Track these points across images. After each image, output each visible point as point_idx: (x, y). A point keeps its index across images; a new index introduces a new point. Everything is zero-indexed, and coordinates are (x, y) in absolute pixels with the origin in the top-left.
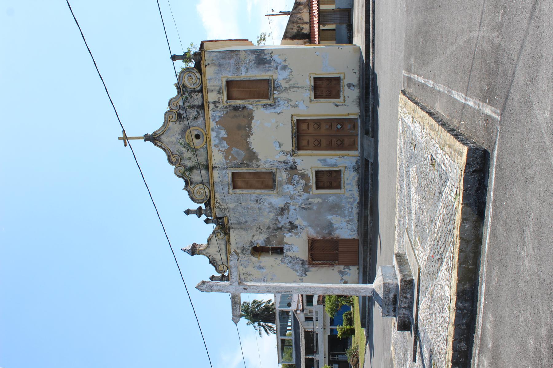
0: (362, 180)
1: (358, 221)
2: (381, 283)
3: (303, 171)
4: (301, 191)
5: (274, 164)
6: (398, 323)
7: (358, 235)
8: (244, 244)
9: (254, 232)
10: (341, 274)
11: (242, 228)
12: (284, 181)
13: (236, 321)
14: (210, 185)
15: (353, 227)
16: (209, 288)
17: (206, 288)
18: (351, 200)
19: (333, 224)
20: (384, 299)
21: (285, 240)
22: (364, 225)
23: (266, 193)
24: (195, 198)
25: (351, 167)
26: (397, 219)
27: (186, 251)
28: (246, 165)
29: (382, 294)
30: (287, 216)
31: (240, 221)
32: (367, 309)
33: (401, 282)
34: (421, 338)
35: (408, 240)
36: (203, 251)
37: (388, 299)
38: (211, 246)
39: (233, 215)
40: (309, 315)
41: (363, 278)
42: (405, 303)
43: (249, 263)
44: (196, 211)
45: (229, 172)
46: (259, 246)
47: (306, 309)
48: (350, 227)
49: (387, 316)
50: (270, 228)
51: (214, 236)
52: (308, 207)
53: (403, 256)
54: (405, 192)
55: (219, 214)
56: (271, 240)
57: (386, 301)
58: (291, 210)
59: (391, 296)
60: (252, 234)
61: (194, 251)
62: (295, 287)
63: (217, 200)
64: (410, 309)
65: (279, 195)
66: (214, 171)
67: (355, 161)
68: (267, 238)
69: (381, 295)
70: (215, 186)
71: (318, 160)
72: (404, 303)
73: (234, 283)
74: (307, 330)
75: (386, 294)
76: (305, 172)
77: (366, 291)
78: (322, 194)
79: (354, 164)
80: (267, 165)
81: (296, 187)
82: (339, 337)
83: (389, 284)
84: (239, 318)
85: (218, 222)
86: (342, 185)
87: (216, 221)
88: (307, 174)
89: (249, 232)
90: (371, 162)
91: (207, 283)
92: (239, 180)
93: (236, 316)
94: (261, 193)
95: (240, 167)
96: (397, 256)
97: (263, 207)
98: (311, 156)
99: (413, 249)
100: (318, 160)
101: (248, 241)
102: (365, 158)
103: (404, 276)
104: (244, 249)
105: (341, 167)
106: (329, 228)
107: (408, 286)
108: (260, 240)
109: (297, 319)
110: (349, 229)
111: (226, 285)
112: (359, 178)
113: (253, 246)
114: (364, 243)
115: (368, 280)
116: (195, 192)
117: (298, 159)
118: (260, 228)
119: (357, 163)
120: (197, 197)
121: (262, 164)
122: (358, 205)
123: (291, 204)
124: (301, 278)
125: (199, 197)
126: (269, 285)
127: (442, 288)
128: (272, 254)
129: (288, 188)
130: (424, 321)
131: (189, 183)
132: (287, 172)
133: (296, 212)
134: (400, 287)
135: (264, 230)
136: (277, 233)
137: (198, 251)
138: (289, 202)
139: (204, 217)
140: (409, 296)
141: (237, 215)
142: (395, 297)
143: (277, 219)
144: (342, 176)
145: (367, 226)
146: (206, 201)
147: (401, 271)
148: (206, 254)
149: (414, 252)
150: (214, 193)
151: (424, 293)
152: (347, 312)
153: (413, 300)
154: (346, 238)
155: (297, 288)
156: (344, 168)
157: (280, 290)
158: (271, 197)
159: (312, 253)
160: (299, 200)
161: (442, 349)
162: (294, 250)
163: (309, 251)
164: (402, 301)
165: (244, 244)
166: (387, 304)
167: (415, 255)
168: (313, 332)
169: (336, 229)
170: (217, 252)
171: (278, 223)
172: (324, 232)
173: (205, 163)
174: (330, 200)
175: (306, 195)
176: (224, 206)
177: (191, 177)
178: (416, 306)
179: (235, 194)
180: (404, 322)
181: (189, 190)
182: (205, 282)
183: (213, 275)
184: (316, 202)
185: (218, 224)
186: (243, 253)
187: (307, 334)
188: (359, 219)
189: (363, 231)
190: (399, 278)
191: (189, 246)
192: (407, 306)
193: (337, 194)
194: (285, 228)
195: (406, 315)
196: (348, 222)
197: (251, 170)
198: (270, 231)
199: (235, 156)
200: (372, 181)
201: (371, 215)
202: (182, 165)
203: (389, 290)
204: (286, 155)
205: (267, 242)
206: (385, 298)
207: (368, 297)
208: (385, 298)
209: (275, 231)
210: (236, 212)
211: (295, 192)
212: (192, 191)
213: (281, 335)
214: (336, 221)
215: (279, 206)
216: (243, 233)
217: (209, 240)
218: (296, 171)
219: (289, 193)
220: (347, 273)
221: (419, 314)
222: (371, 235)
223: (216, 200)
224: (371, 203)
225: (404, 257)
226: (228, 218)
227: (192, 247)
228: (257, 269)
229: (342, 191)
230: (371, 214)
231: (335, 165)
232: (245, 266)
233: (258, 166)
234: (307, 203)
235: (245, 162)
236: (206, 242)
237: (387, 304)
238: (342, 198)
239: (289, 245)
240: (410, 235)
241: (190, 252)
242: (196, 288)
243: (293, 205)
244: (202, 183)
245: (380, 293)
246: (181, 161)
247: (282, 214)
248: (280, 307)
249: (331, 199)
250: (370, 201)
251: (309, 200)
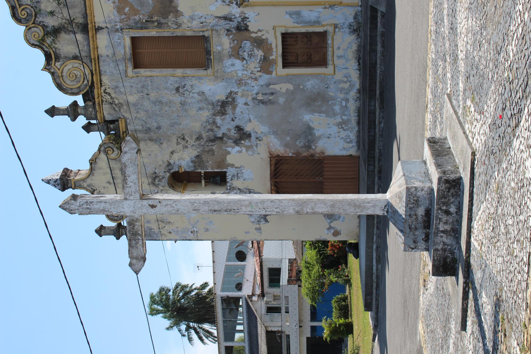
0: (364, 47)
1: (358, 123)
2: (403, 187)
3: (259, 34)
4: (256, 70)
5: (208, 21)
6: (434, 261)
7: (359, 148)
8: (155, 168)
9: (173, 146)
10: (329, 219)
11: (151, 140)
12: (225, 52)
13: (136, 267)
14: (91, 61)
15: (350, 134)
16: (85, 206)
17: (80, 206)
18: (346, 86)
19: (313, 129)
20: (408, 217)
21: (230, 159)
22: (369, 128)
23: (193, 75)
24: (65, 86)
25: (346, 26)
26: (430, 90)
27: (52, 182)
28: (156, 24)
29: (404, 209)
30: (232, 116)
31: (148, 126)
32: (374, 277)
33: (439, 184)
34: (476, 282)
35: (452, 111)
36: (81, 183)
37: (414, 217)
38: (96, 173)
39: (135, 115)
40: (274, 304)
41: (367, 223)
42: (446, 223)
44: (67, 109)
45: (126, 37)
46: (183, 170)
47: (267, 293)
48: (343, 134)
49: (413, 249)
50: (202, 138)
51: (102, 153)
52: (270, 100)
53: (441, 143)
54: (445, 30)
55: (109, 114)
56: (203, 159)
57: (412, 222)
58: (239, 105)
59: (421, 211)
60: (171, 150)
61: (65, 181)
62: (244, 200)
63: (106, 89)
64: (455, 235)
65: (216, 77)
66: (98, 36)
67: (353, 14)
68: (197, 157)
69: (402, 210)
70: (101, 64)
71: (286, 12)
72: (444, 223)
73: (131, 195)
74: (270, 329)
75: (411, 208)
76: (263, 35)
77: (374, 206)
78: (294, 75)
79: (351, 20)
80: (194, 23)
81: (247, 63)
82: (326, 339)
83: (416, 188)
84: (142, 263)
85: (108, 128)
86: (329, 58)
87: (105, 127)
88: (267, 39)
89: (164, 145)
90: (382, 12)
91: (82, 197)
92: (144, 51)
93: (137, 258)
94: (185, 75)
95: (146, 28)
96: (430, 142)
97: (189, 101)
98: (274, 5)
99: (460, 123)
100: (286, 12)
101: (163, 162)
102: (370, 5)
103: (444, 172)
104: (156, 177)
105: (327, 25)
106: (306, 136)
107: (452, 191)
108: (184, 160)
109: (253, 311)
110: (342, 138)
111: (116, 201)
112: (359, 46)
113: (172, 171)
114: (368, 161)
115: (375, 225)
116: (64, 74)
117: (250, 13)
118: (184, 139)
119: (355, 17)
120: (68, 83)
121: (185, 21)
122: (358, 95)
123: (239, 94)
124: (258, 226)
125: (72, 84)
126: (197, 197)
127: (520, 166)
128: (205, 186)
129: (233, 65)
130: (483, 247)
131: (53, 57)
132: (231, 37)
133: (247, 109)
134: (437, 192)
135: (191, 142)
136: (214, 148)
137: (73, 183)
138: (235, 90)
139: (82, 120)
140: (453, 209)
141: (142, 115)
142: (428, 213)
143: (214, 123)
144: (330, 42)
145: (375, 128)
146: (85, 91)
147: (438, 165)
148: (88, 188)
149: (463, 128)
150: (100, 75)
151: (482, 197)
152: (340, 296)
153: (461, 217)
154: (337, 154)
155: (247, 203)
156: (333, 27)
157: (216, 208)
158: (203, 81)
159: (276, 182)
160: (254, 86)
161: (519, 283)
162: (245, 176)
163: (271, 178)
164: (440, 219)
165: (155, 168)
166: (413, 226)
167: (465, 133)
168: (281, 332)
169: (320, 137)
170: (109, 182)
171: (216, 129)
172: (297, 143)
173: (81, 20)
174: (309, 87)
175: (265, 78)
176: (120, 99)
177: (56, 46)
178: (468, 225)
179: (137, 76)
180: (445, 259)
181: (52, 71)
182: (78, 196)
183: (102, 226)
184: (284, 90)
185: (107, 133)
186: (154, 184)
187: (271, 336)
188: (359, 119)
189: (367, 139)
190: (435, 175)
191: (56, 173)
192: (449, 229)
193: (319, 74)
194: (229, 138)
195: (448, 245)
196: (341, 125)
197: (166, 33)
198: (202, 144)
199: (136, 7)
200: (383, 46)
201: (380, 109)
202: (39, 25)
203: (417, 201)
204: (229, 5)
205: (197, 164)
206: (410, 215)
207: (378, 216)
208: (410, 215)
209: (211, 144)
210: (139, 110)
211: (245, 72)
212: (59, 72)
213: (226, 340)
214: (319, 123)
215: (217, 98)
216: (154, 147)
217: (93, 162)
218: (246, 33)
219: (235, 74)
220: (339, 217)
221: (472, 239)
222: (381, 144)
223: (103, 88)
224: (380, 87)
225: (444, 143)
226: (126, 122)
227: (62, 175)
229: (329, 70)
230: (382, 107)
231: (317, 23)
233: (179, 25)
234: (267, 92)
235: (155, 18)
236: (88, 167)
237: (413, 226)
238: (329, 82)
239: (236, 168)
240: (454, 102)
241: (58, 184)
242: (60, 207)
243: (242, 96)
244: (75, 58)
245: (400, 208)
246: (36, 16)
247: (223, 113)
248: (223, 290)
249: (310, 84)
250: (380, 83)
251: (271, 86)
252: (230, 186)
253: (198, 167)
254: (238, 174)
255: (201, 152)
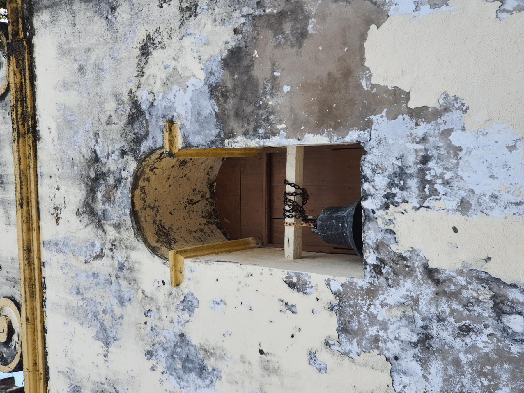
43: (121, 301)
60: (141, 36)
128: (298, 257)
186: (92, 212)
205: (231, 102)
228: (170, 369)
232: (103, 328)
252: (377, 248)
253: (234, 124)
254: (425, 160)
255: (248, 28)
